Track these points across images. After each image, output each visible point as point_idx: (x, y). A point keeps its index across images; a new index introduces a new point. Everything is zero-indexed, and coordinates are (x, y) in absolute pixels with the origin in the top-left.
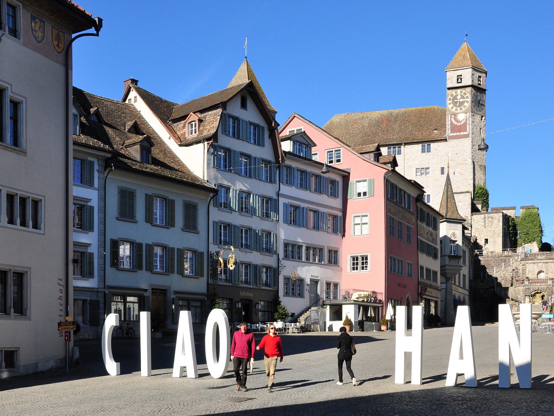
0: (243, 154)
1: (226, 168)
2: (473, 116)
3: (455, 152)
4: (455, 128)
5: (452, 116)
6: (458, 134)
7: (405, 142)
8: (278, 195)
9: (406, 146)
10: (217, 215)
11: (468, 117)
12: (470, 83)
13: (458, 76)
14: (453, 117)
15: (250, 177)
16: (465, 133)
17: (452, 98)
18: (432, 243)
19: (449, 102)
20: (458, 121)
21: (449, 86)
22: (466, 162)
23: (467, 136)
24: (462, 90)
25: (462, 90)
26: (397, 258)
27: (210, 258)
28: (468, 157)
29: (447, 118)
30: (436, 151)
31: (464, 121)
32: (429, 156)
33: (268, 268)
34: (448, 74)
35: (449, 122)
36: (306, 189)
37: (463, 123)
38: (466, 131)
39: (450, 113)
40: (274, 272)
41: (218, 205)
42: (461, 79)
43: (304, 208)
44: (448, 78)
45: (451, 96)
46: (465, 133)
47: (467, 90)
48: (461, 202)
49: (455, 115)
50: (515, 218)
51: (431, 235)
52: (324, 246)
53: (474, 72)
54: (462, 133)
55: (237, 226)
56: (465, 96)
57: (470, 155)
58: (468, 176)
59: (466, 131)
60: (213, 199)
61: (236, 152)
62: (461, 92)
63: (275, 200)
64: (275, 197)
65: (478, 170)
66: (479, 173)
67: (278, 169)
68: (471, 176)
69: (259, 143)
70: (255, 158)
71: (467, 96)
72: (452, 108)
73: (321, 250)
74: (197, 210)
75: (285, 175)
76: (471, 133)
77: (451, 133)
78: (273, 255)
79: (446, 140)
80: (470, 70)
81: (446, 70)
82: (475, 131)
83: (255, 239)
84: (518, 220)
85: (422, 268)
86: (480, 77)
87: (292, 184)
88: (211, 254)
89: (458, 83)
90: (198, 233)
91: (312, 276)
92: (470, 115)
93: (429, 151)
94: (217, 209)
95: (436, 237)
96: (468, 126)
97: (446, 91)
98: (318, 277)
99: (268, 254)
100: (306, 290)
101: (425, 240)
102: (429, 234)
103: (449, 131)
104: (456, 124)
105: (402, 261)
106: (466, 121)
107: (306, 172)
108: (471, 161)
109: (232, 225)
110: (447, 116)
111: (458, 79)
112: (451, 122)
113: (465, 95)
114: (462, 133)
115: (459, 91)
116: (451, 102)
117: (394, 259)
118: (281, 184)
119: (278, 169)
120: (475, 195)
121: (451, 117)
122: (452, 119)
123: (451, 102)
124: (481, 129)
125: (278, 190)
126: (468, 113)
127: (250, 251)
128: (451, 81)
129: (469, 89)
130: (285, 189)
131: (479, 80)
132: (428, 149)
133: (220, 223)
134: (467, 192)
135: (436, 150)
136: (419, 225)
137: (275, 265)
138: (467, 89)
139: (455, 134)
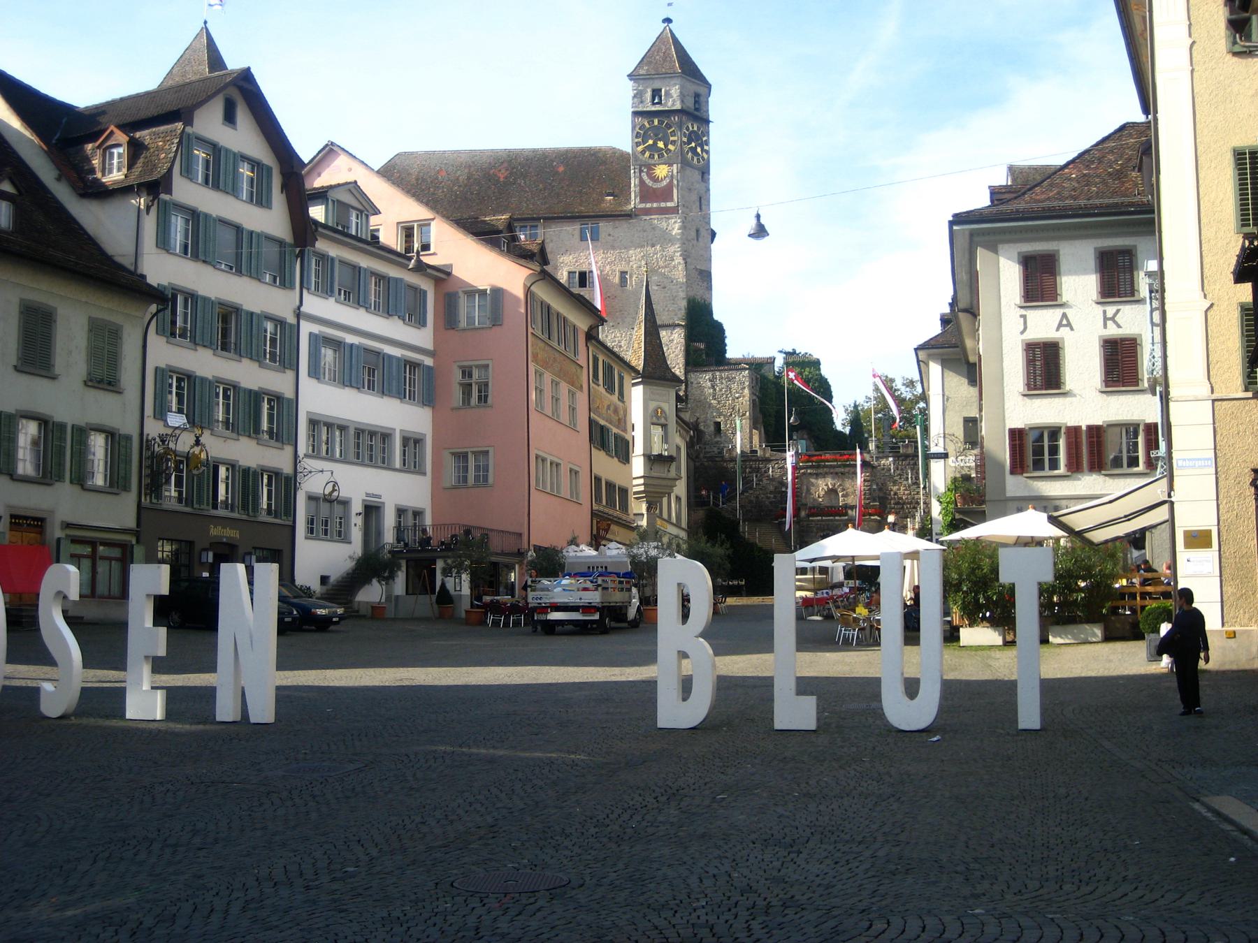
0: (223, 222)
1: (186, 253)
4: (647, 194)
6: (655, 205)
8: (299, 315)
10: (163, 353)
12: (678, 106)
14: (645, 170)
15: (239, 272)
16: (669, 204)
18: (618, 427)
19: (636, 140)
20: (656, 180)
23: (674, 211)
26: (549, 458)
27: (147, 449)
28: (678, 254)
29: (632, 171)
30: (611, 238)
33: (275, 475)
36: (359, 304)
37: (664, 183)
38: (672, 200)
40: (286, 485)
41: (170, 332)
43: (352, 345)
45: (640, 129)
46: (669, 204)
49: (650, 168)
51: (616, 411)
52: (395, 430)
54: (663, 205)
55: (206, 379)
56: (669, 131)
59: (672, 200)
60: (155, 317)
61: (211, 216)
62: (660, 122)
63: (291, 325)
64: (291, 320)
67: (299, 259)
69: (260, 199)
70: (251, 233)
72: (643, 152)
73: (386, 436)
74: (119, 341)
75: (313, 271)
77: (642, 201)
78: (285, 447)
79: (629, 216)
83: (247, 410)
85: (598, 479)
86: (697, 96)
87: (329, 293)
88: (147, 441)
89: (654, 104)
90: (120, 393)
91: (368, 495)
94: (165, 339)
95: (625, 416)
96: (675, 191)
98: (379, 497)
99: (273, 442)
100: (355, 525)
101: (602, 422)
102: (612, 408)
104: (650, 185)
105: (558, 465)
106: (671, 181)
107: (357, 269)
109: (196, 377)
111: (653, 98)
112: (642, 182)
113: (669, 129)
114: (663, 205)
117: (544, 460)
118: (305, 292)
119: (299, 259)
121: (641, 171)
123: (640, 140)
124: (700, 198)
125: (298, 303)
126: (675, 166)
127: (234, 435)
130: (315, 304)
131: (696, 102)
133: (170, 371)
135: (609, 235)
136: (591, 390)
137: (287, 469)
139: (649, 205)
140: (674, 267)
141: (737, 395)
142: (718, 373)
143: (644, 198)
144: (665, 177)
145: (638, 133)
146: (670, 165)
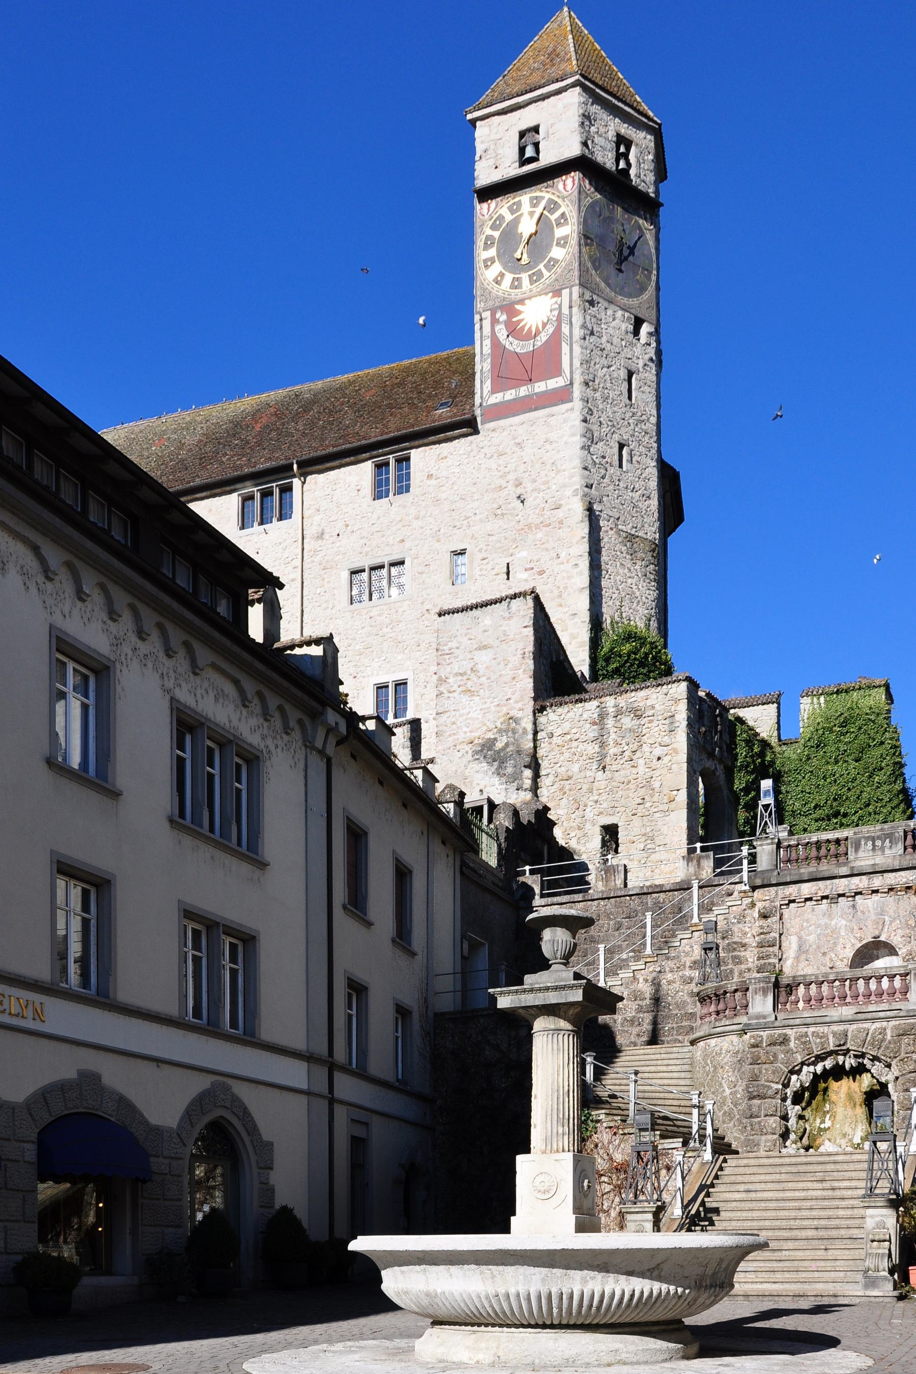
2: (592, 303)
3: (511, 477)
5: (497, 316)
6: (523, 391)
7: (307, 454)
9: (309, 478)
11: (566, 310)
13: (522, 134)
14: (503, 318)
17: (496, 234)
21: (485, 175)
22: (560, 514)
23: (562, 396)
24: (538, 194)
25: (538, 194)
29: (477, 327)
30: (433, 482)
31: (550, 329)
32: (404, 507)
34: (481, 130)
35: (487, 343)
38: (558, 372)
39: (490, 303)
42: (536, 145)
44: (479, 147)
47: (561, 186)
48: (485, 647)
50: (774, 741)
53: (595, 109)
54: (540, 387)
57: (577, 481)
58: (569, 578)
62: (535, 202)
65: (615, 558)
66: (621, 571)
68: (581, 573)
71: (563, 214)
76: (578, 379)
77: (494, 391)
80: (574, 96)
81: (469, 117)
82: (600, 373)
84: (788, 751)
92: (575, 295)
93: (403, 487)
97: (473, 208)
103: (488, 385)
108: (578, 509)
110: (477, 318)
111: (522, 150)
113: (552, 211)
114: (540, 387)
115: (525, 198)
116: (492, 252)
120: (601, 663)
122: (497, 328)
128: (491, 162)
129: (569, 182)
132: (399, 479)
134: (515, 596)
135: (430, 476)
138: (559, 183)
139: (510, 395)
140: (561, 522)
141: (658, 751)
142: (610, 702)
143: (500, 381)
144: (544, 325)
145: (488, 238)
146: (557, 293)
